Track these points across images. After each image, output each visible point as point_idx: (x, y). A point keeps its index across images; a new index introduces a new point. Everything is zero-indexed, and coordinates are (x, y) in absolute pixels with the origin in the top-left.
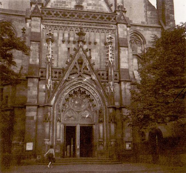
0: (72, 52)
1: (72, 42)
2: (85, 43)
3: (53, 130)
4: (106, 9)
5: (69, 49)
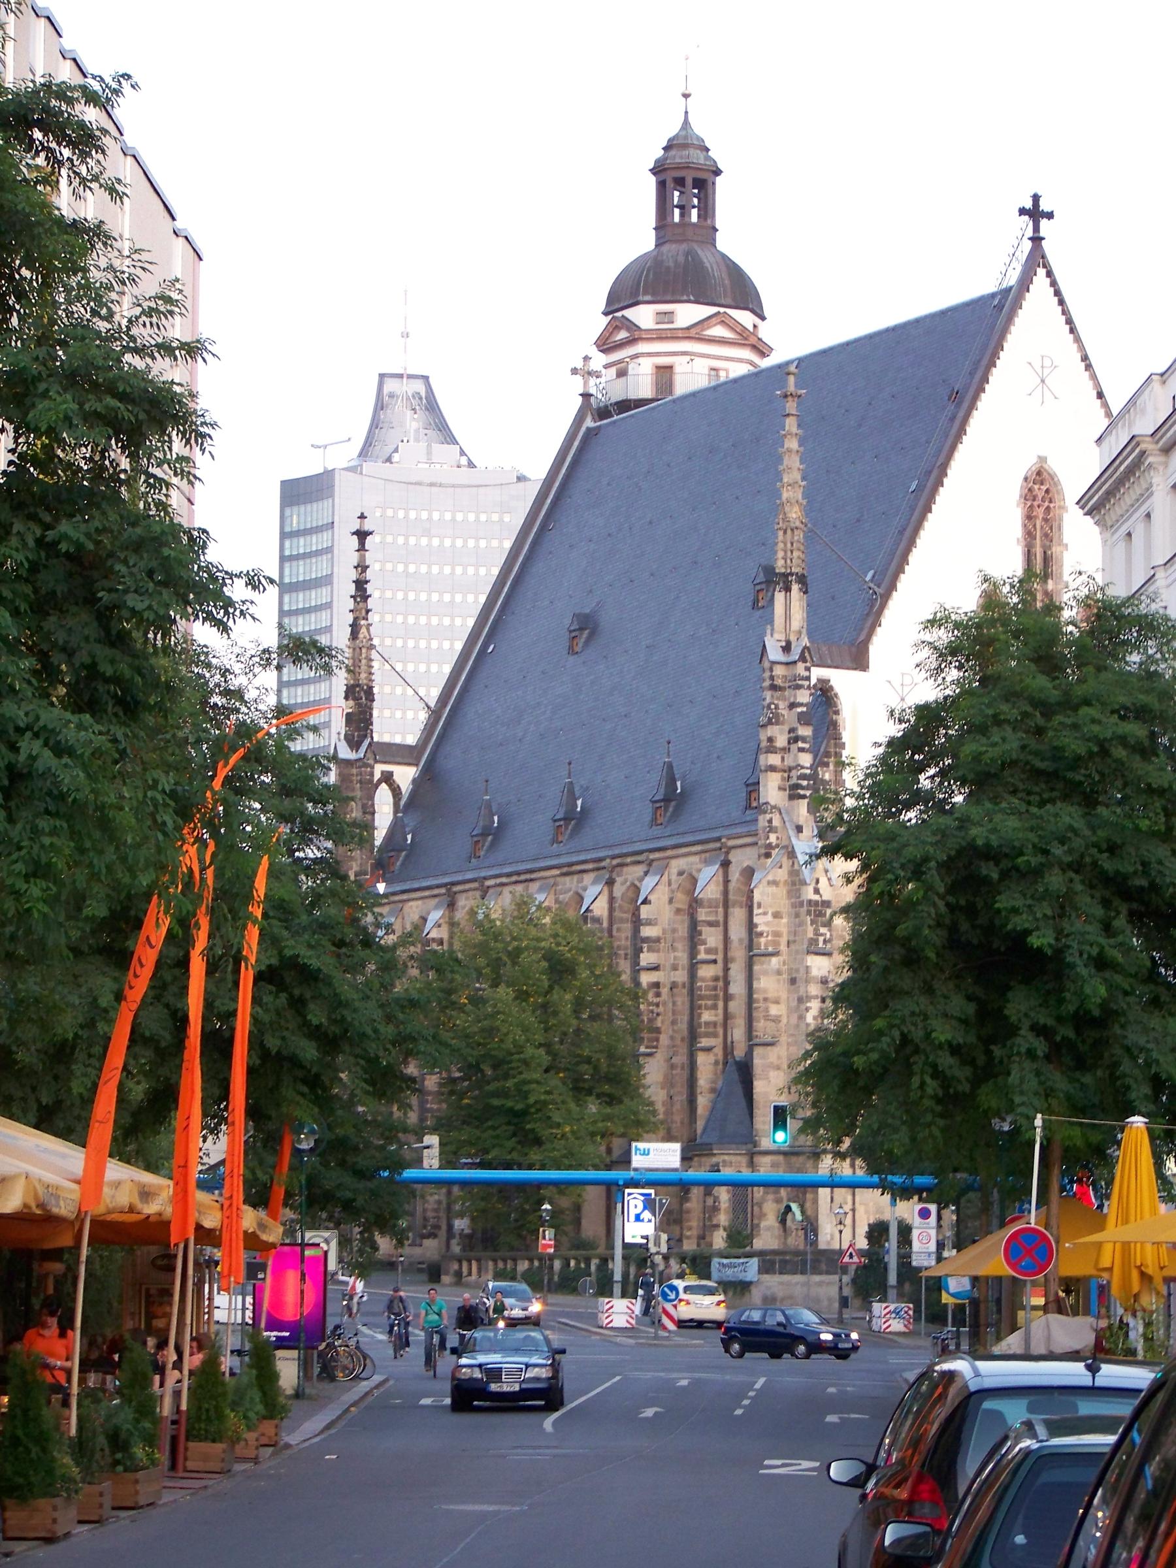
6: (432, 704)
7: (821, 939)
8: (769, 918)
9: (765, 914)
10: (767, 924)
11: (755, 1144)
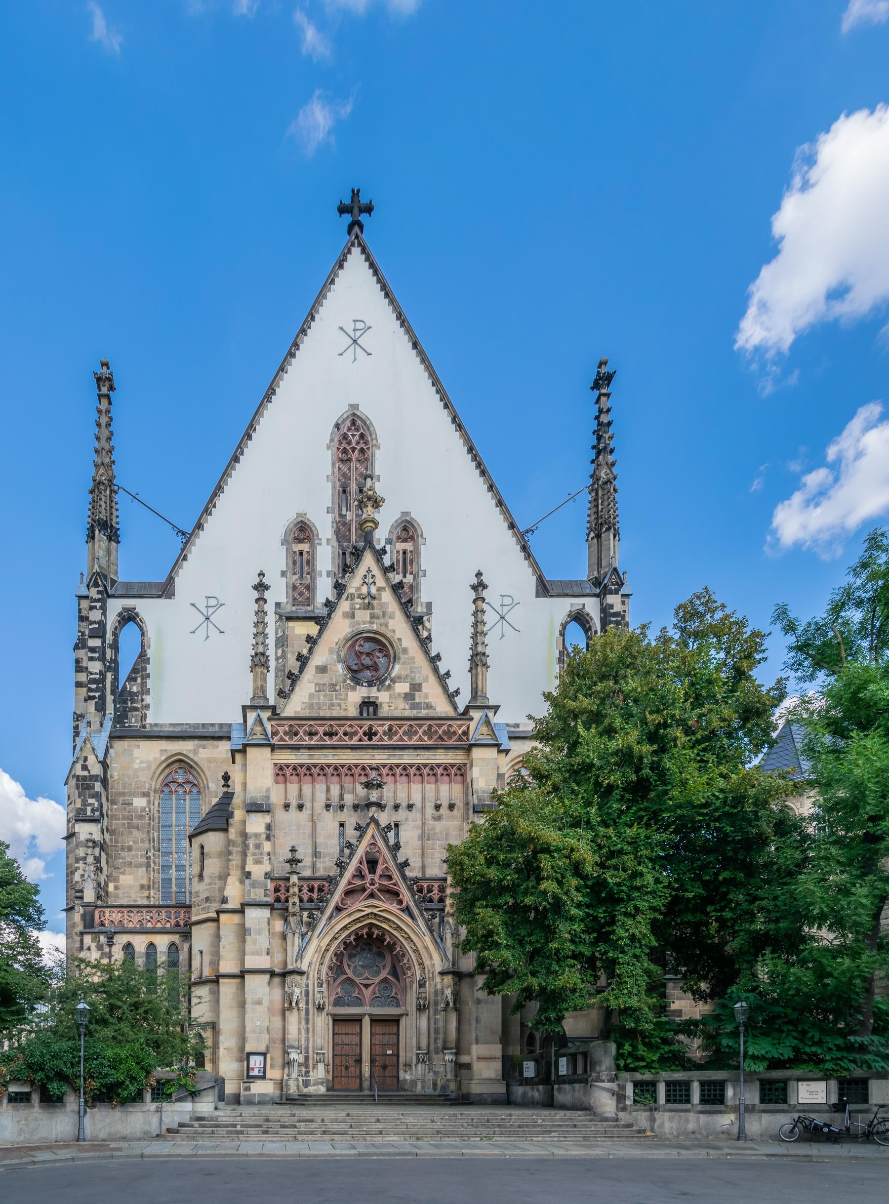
0: (351, 833)
1: (351, 808)
2: (385, 807)
3: (307, 1030)
4: (442, 708)
5: (342, 825)
7: (89, 808)
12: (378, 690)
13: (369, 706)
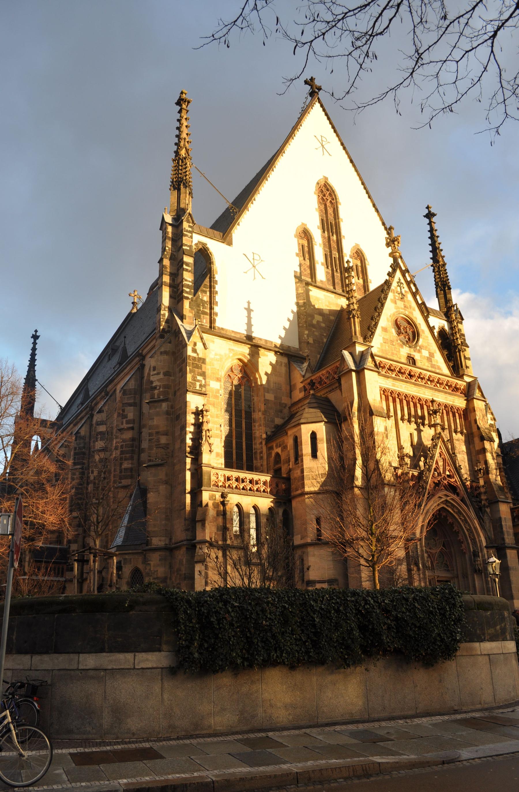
6: (63, 406)
7: (198, 384)
8: (161, 376)
9: (158, 374)
10: (159, 380)
11: (148, 543)
12: (415, 351)
13: (412, 361)
